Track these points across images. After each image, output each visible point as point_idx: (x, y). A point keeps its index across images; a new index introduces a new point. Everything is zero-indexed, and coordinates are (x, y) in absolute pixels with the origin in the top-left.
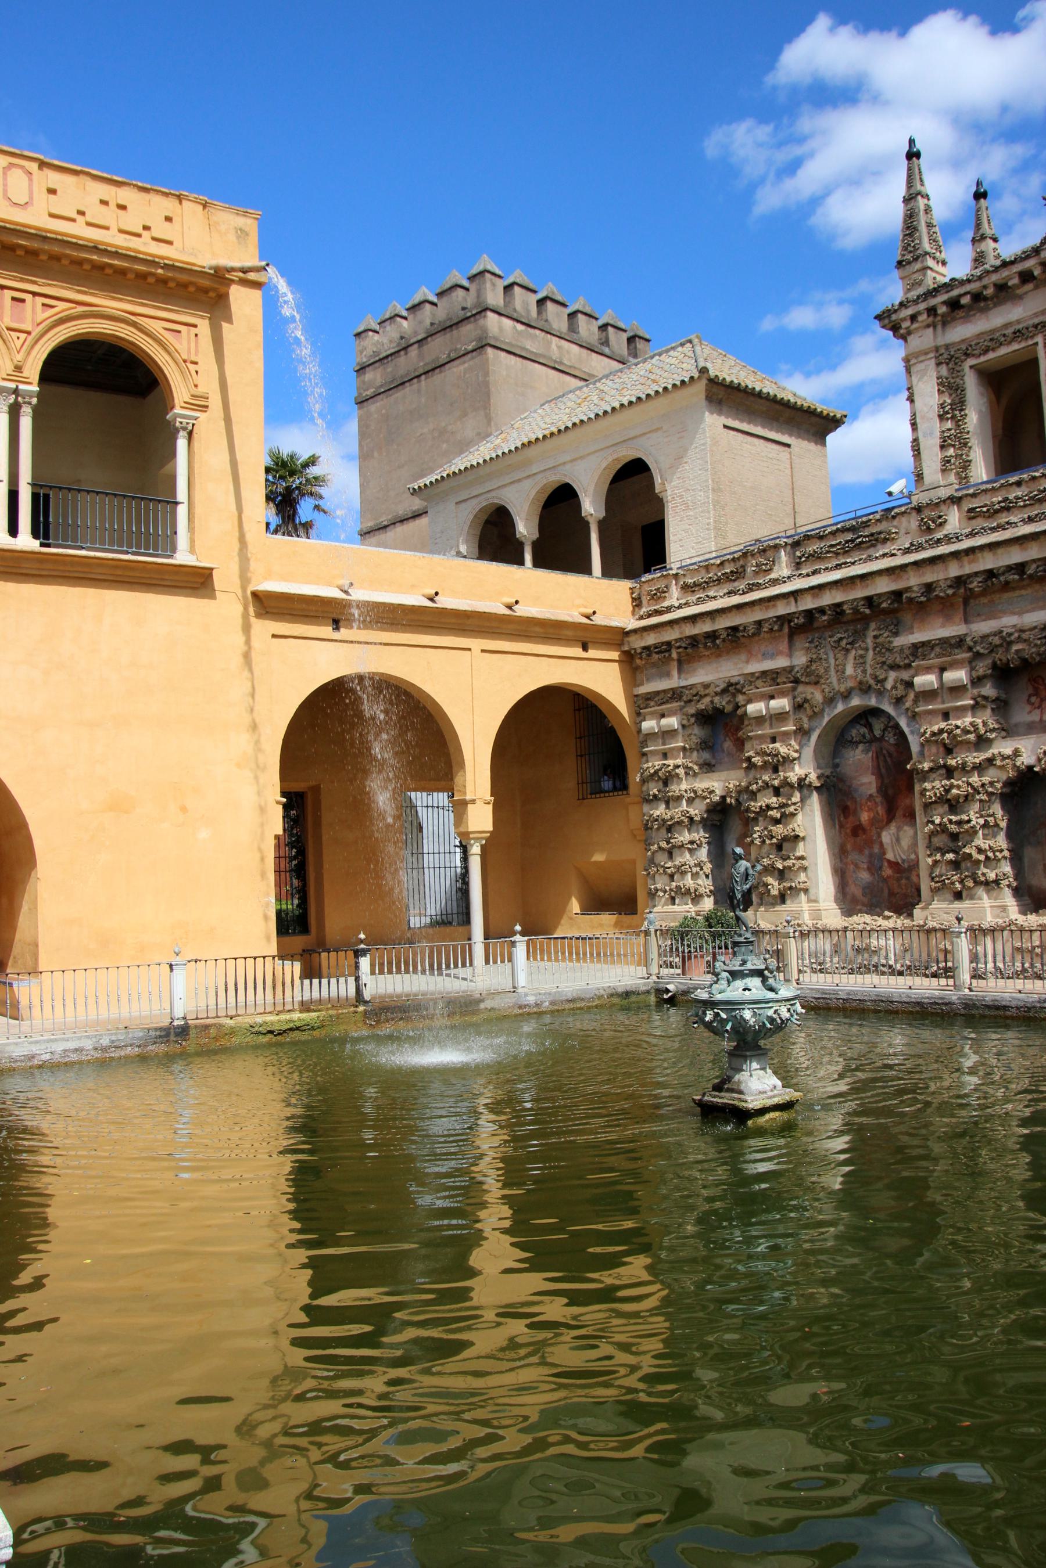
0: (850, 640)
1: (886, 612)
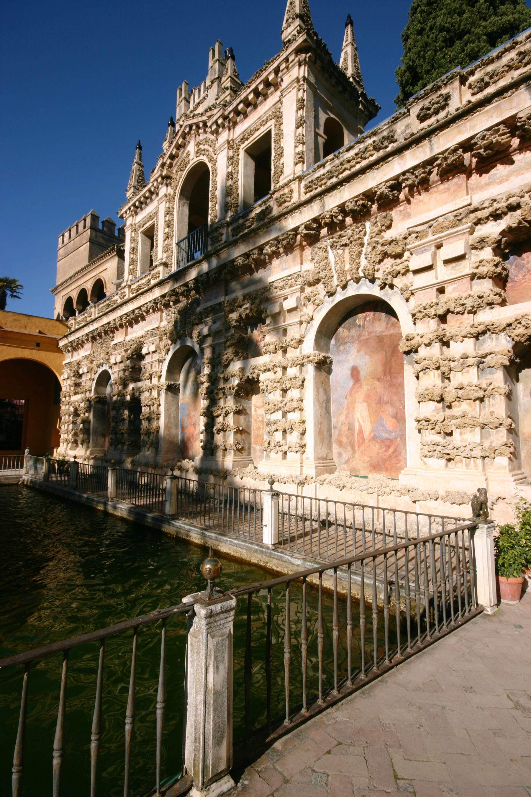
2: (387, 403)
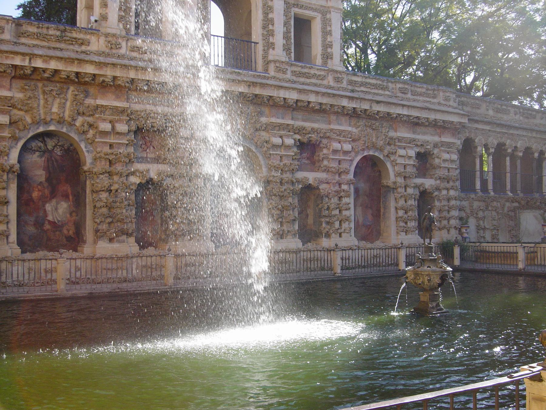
0: (58, 92)
1: (86, 83)
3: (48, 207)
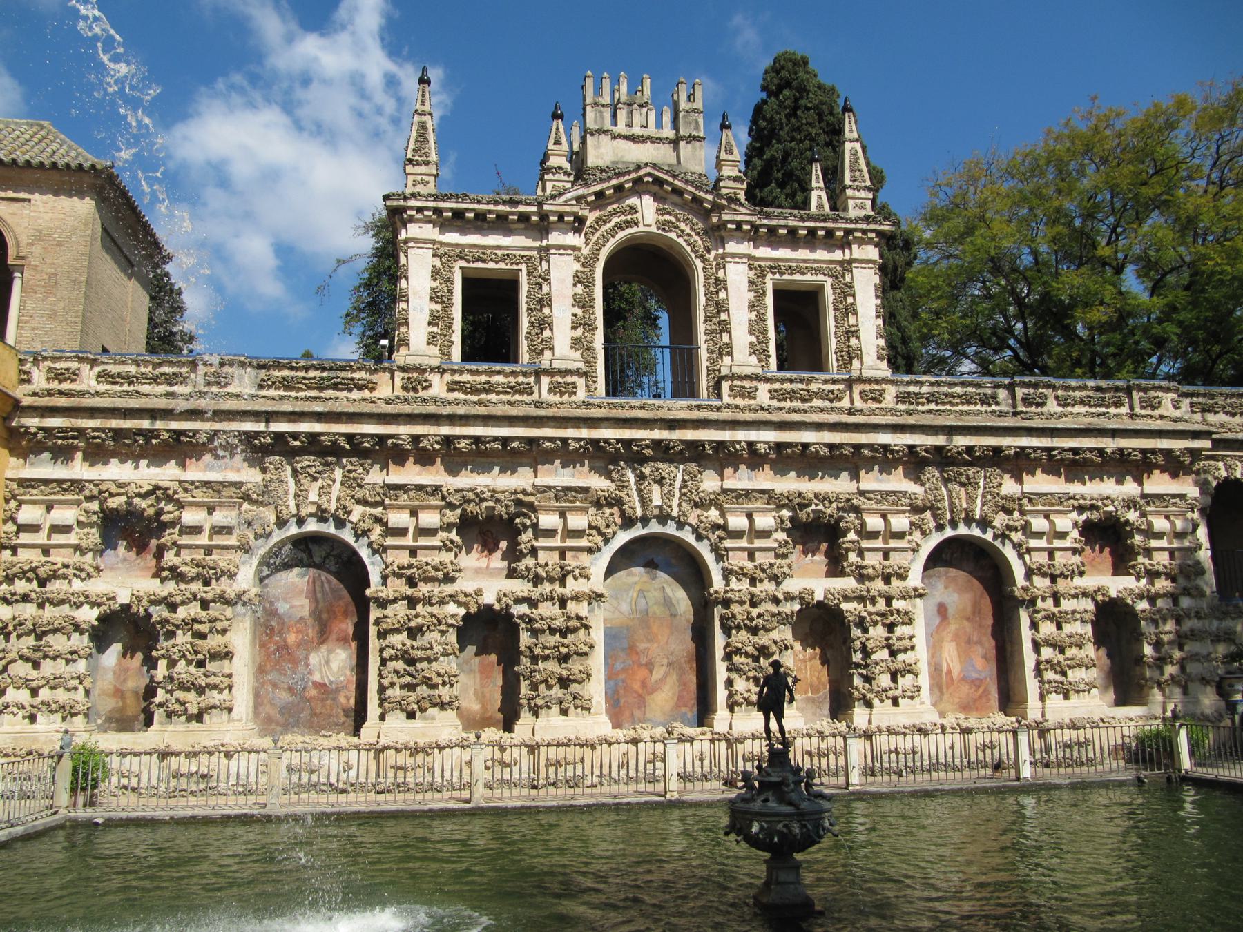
0: (320, 468)
2: (976, 643)
3: (314, 659)
